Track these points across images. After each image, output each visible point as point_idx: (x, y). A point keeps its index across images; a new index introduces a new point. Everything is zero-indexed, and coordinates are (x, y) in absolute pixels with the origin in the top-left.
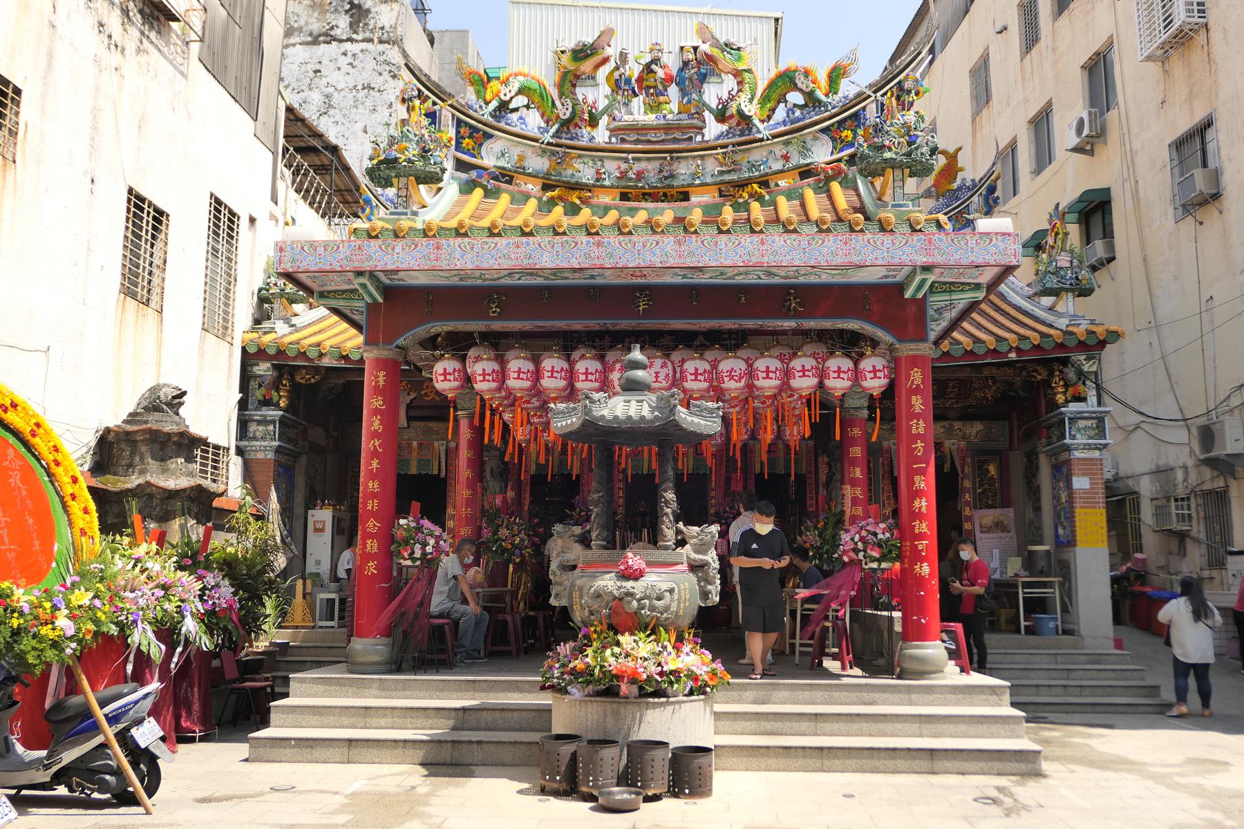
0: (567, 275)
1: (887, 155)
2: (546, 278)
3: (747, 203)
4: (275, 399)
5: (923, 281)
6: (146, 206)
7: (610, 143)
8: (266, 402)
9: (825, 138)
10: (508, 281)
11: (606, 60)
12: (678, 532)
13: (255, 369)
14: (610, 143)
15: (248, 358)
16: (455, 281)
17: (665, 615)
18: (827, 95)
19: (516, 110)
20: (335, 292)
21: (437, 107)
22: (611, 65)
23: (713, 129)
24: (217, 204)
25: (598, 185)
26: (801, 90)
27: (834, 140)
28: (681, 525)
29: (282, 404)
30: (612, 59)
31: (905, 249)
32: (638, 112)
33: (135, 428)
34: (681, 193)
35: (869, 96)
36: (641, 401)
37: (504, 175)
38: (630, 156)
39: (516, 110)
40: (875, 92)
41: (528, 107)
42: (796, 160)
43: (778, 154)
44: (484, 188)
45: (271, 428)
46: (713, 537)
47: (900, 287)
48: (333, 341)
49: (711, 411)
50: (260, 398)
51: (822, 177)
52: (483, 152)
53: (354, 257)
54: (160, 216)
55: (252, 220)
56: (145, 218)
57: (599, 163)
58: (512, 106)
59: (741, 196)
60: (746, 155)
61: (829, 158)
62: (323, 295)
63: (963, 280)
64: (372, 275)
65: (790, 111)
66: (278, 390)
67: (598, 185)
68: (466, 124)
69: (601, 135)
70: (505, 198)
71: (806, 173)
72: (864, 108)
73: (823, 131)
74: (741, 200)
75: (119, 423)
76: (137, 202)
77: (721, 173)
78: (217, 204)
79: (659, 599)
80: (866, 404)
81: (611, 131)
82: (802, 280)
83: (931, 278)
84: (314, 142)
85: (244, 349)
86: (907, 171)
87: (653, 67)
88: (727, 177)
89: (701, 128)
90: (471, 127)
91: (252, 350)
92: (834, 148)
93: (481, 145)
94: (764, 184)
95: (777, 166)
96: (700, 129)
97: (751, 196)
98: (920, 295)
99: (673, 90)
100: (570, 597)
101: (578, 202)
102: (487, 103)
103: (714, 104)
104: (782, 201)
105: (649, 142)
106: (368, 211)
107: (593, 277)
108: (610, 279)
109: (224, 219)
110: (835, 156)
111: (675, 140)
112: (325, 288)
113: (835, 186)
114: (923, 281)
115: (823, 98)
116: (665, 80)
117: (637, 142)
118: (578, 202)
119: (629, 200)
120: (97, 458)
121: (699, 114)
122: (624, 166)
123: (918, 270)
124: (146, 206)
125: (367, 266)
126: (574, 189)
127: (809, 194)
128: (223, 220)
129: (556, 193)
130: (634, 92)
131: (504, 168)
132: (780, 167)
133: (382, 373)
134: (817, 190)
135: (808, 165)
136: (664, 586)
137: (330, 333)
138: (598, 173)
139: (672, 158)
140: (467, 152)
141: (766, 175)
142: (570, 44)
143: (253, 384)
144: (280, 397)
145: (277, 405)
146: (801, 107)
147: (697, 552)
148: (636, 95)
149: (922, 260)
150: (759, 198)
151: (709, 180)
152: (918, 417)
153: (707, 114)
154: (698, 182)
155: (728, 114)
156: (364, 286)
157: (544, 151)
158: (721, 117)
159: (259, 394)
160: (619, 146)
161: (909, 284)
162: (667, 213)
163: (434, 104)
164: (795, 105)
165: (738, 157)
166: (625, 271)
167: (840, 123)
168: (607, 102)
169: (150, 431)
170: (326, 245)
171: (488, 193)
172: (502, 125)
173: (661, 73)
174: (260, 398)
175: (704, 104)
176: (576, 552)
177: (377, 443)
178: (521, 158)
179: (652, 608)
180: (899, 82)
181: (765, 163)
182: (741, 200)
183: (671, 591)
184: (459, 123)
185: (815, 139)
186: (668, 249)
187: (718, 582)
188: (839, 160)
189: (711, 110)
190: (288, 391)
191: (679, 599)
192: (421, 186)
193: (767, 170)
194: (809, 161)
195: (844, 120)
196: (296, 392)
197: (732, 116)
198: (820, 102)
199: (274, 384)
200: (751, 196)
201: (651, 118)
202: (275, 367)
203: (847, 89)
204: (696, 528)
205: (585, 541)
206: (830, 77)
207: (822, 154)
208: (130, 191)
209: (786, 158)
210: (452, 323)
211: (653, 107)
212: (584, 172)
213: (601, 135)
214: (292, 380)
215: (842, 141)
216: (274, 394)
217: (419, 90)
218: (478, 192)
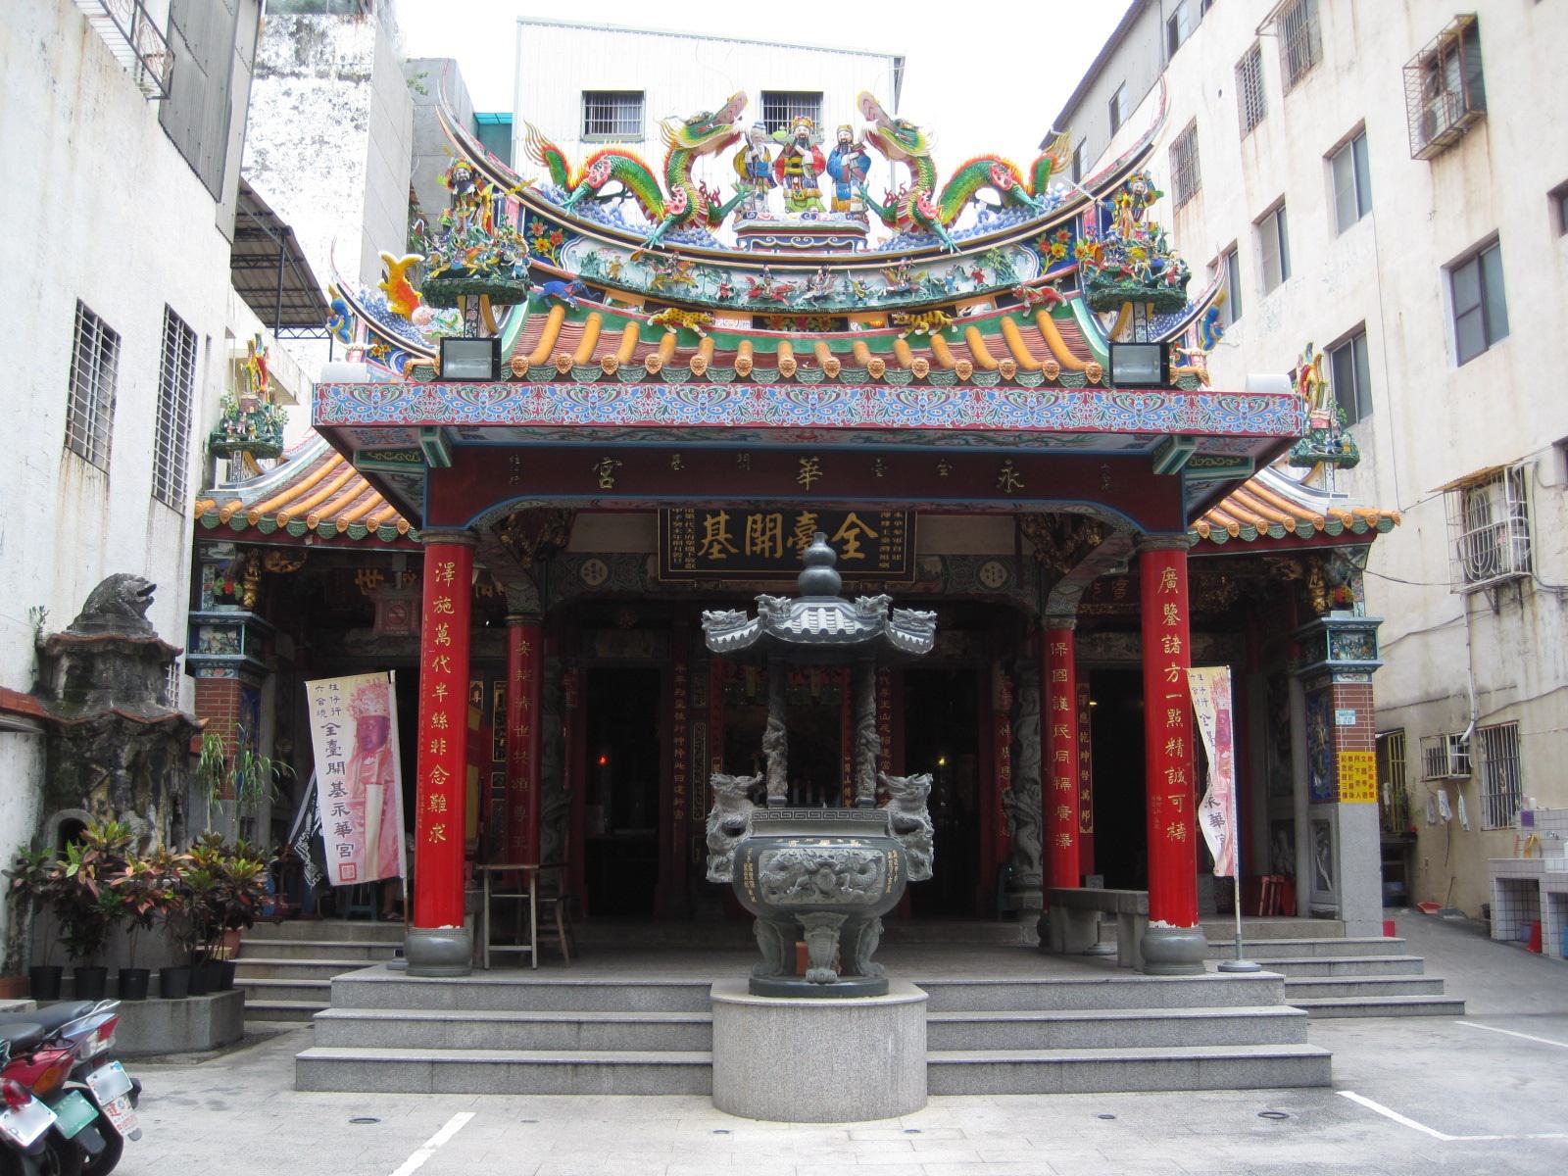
0: (709, 435)
1: (1128, 285)
2: (679, 438)
3: (926, 337)
4: (238, 595)
5: (1182, 453)
6: (95, 327)
7: (738, 249)
8: (226, 599)
9: (1031, 254)
10: (628, 442)
11: (733, 139)
12: (880, 783)
13: (212, 551)
14: (738, 249)
15: (206, 533)
16: (553, 440)
17: (870, 893)
18: (1033, 196)
19: (607, 199)
20: (383, 451)
21: (500, 195)
22: (742, 144)
23: (879, 236)
24: (172, 317)
25: (724, 305)
26: (998, 187)
27: (1041, 255)
28: (883, 775)
29: (247, 602)
30: (743, 136)
31: (1162, 412)
32: (776, 208)
33: (93, 636)
34: (836, 319)
35: (1087, 200)
36: (832, 609)
37: (592, 290)
38: (768, 267)
39: (607, 199)
40: (1095, 193)
41: (622, 195)
42: (990, 280)
43: (969, 272)
44: (566, 305)
45: (233, 635)
46: (926, 789)
47: (1148, 461)
48: (323, 512)
49: (922, 622)
50: (218, 592)
51: (1027, 304)
52: (563, 258)
53: (423, 407)
54: (110, 337)
55: (208, 339)
56: (94, 339)
57: (725, 276)
58: (603, 193)
59: (919, 327)
60: (926, 271)
61: (1036, 280)
62: (364, 456)
63: (1228, 453)
64: (445, 430)
65: (982, 215)
66: (241, 581)
67: (724, 305)
68: (540, 217)
69: (725, 237)
70: (594, 319)
71: (1005, 297)
72: (1080, 215)
73: (1028, 242)
74: (918, 332)
75: (65, 629)
76: (85, 318)
77: (892, 294)
78: (172, 317)
79: (863, 871)
80: (1074, 611)
81: (741, 232)
82: (1023, 447)
83: (1193, 449)
84: (260, 222)
85: (197, 523)
86: (1151, 306)
87: (798, 148)
88: (898, 301)
89: (863, 233)
90: (547, 221)
91: (208, 525)
92: (1042, 266)
93: (560, 247)
94: (951, 310)
95: (966, 287)
96: (861, 233)
97: (933, 326)
98: (1174, 472)
99: (825, 182)
100: (739, 870)
101: (696, 328)
102: (570, 191)
103: (879, 199)
104: (973, 333)
105: (792, 248)
106: (341, 322)
107: (744, 438)
108: (766, 441)
109: (179, 340)
110: (1044, 277)
111: (828, 247)
112: (371, 447)
113: (1044, 317)
114: (1182, 453)
115: (1027, 199)
116: (813, 165)
117: (776, 247)
118: (696, 328)
119: (765, 327)
120: (36, 676)
121: (862, 216)
122: (759, 280)
123: (1176, 439)
124: (95, 327)
125: (441, 418)
126: (689, 310)
127: (1011, 326)
128: (178, 337)
129: (667, 313)
130: (771, 180)
131: (591, 280)
132: (971, 290)
133: (450, 565)
134: (1021, 321)
135: (1008, 287)
136: (869, 855)
137: (342, 499)
138: (723, 288)
139: (825, 272)
140: (541, 257)
141: (954, 298)
142: (692, 112)
143: (207, 572)
144: (245, 591)
145: (240, 602)
146: (996, 209)
147: (905, 809)
148: (774, 185)
149: (1181, 427)
150: (945, 330)
151: (874, 303)
152: (1172, 631)
153: (871, 214)
154: (860, 305)
155: (899, 215)
156: (432, 446)
157: (647, 257)
158: (890, 219)
159: (218, 586)
160: (752, 252)
161: (1162, 457)
162: (824, 349)
163: (496, 190)
164: (990, 207)
165: (914, 274)
166: (790, 432)
167: (1050, 232)
168: (734, 194)
169: (112, 640)
170: (366, 388)
171: (570, 313)
172: (590, 220)
173: (808, 157)
174: (218, 592)
175: (869, 201)
176: (745, 812)
177: (443, 662)
178: (617, 267)
179: (854, 885)
180: (1126, 184)
181: (949, 283)
182: (918, 332)
183: (877, 861)
184: (530, 214)
185: (1017, 253)
186: (853, 404)
187: (932, 849)
188: (1050, 282)
189: (875, 208)
190: (256, 583)
191: (887, 871)
192: (494, 308)
193: (954, 293)
194: (1010, 282)
195: (1054, 230)
196: (269, 586)
197: (905, 219)
198: (1022, 203)
199: (237, 573)
200: (933, 326)
201: (794, 219)
202: (239, 548)
203: (1059, 187)
204: (902, 779)
205: (758, 796)
206: (1035, 170)
207: (1026, 271)
208: (79, 303)
209: (978, 276)
210: (547, 498)
211: (798, 201)
212: (704, 287)
213: (725, 237)
214: (261, 567)
215: (1052, 257)
216: (237, 587)
217: (474, 171)
218: (557, 313)
